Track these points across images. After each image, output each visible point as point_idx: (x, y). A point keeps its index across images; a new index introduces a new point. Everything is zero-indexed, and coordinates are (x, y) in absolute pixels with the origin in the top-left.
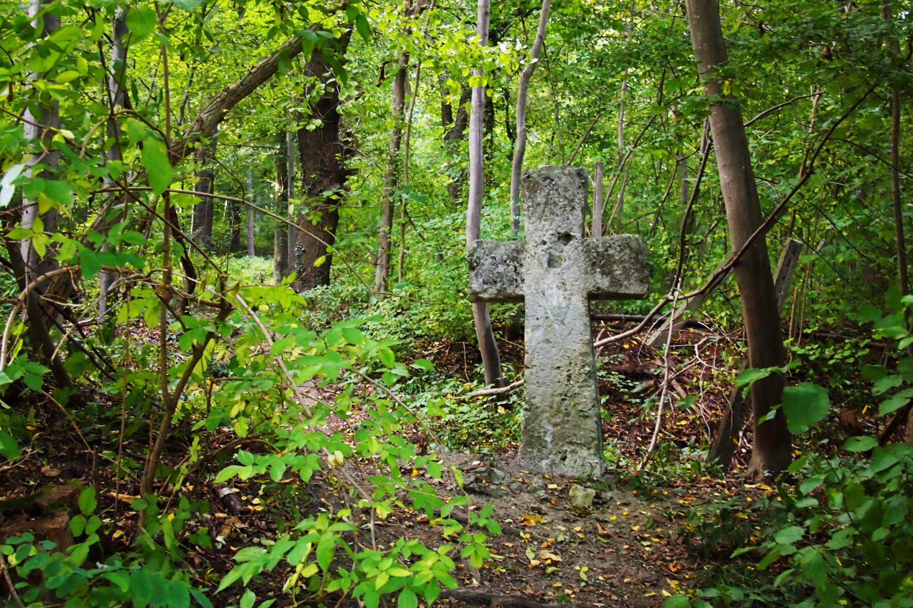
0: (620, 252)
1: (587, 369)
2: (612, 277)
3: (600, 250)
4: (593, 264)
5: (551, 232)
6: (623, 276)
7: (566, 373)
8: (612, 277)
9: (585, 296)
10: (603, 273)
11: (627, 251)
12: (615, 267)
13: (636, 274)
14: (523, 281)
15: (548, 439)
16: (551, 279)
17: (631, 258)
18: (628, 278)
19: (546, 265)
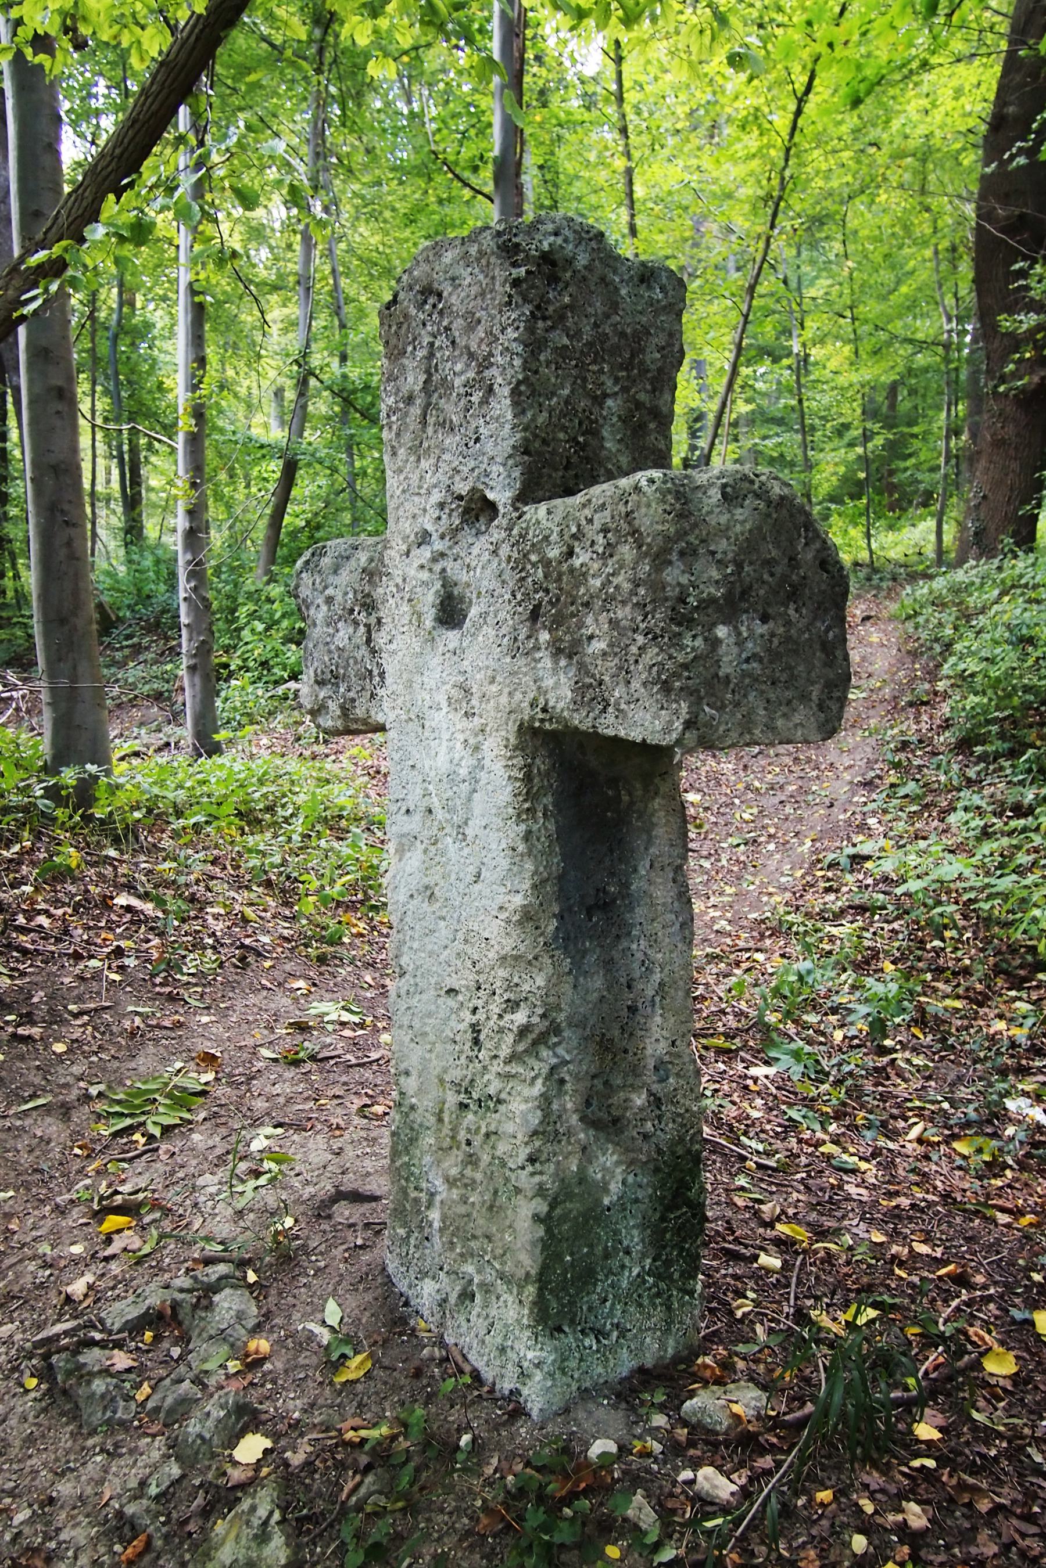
0: (605, 557)
1: (520, 1017)
2: (582, 667)
3: (553, 553)
4: (535, 615)
5: (436, 497)
6: (613, 663)
7: (468, 1018)
8: (582, 667)
9: (513, 741)
10: (557, 651)
11: (626, 551)
12: (591, 626)
13: (652, 655)
14: (382, 675)
15: (435, 1215)
16: (436, 679)
17: (636, 583)
18: (624, 672)
19: (429, 623)
